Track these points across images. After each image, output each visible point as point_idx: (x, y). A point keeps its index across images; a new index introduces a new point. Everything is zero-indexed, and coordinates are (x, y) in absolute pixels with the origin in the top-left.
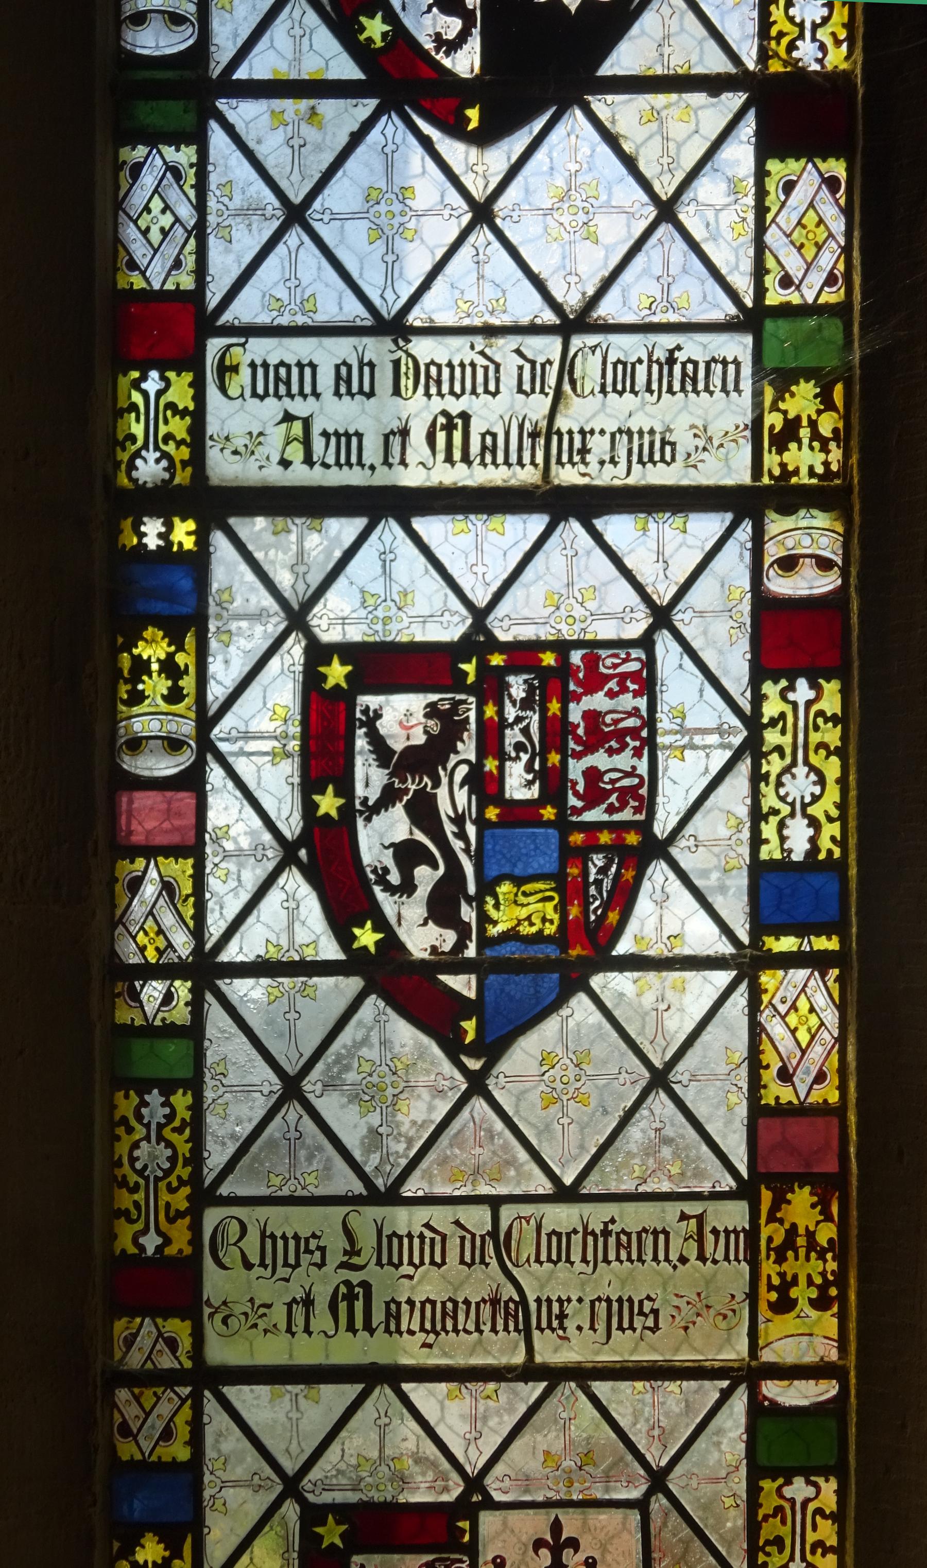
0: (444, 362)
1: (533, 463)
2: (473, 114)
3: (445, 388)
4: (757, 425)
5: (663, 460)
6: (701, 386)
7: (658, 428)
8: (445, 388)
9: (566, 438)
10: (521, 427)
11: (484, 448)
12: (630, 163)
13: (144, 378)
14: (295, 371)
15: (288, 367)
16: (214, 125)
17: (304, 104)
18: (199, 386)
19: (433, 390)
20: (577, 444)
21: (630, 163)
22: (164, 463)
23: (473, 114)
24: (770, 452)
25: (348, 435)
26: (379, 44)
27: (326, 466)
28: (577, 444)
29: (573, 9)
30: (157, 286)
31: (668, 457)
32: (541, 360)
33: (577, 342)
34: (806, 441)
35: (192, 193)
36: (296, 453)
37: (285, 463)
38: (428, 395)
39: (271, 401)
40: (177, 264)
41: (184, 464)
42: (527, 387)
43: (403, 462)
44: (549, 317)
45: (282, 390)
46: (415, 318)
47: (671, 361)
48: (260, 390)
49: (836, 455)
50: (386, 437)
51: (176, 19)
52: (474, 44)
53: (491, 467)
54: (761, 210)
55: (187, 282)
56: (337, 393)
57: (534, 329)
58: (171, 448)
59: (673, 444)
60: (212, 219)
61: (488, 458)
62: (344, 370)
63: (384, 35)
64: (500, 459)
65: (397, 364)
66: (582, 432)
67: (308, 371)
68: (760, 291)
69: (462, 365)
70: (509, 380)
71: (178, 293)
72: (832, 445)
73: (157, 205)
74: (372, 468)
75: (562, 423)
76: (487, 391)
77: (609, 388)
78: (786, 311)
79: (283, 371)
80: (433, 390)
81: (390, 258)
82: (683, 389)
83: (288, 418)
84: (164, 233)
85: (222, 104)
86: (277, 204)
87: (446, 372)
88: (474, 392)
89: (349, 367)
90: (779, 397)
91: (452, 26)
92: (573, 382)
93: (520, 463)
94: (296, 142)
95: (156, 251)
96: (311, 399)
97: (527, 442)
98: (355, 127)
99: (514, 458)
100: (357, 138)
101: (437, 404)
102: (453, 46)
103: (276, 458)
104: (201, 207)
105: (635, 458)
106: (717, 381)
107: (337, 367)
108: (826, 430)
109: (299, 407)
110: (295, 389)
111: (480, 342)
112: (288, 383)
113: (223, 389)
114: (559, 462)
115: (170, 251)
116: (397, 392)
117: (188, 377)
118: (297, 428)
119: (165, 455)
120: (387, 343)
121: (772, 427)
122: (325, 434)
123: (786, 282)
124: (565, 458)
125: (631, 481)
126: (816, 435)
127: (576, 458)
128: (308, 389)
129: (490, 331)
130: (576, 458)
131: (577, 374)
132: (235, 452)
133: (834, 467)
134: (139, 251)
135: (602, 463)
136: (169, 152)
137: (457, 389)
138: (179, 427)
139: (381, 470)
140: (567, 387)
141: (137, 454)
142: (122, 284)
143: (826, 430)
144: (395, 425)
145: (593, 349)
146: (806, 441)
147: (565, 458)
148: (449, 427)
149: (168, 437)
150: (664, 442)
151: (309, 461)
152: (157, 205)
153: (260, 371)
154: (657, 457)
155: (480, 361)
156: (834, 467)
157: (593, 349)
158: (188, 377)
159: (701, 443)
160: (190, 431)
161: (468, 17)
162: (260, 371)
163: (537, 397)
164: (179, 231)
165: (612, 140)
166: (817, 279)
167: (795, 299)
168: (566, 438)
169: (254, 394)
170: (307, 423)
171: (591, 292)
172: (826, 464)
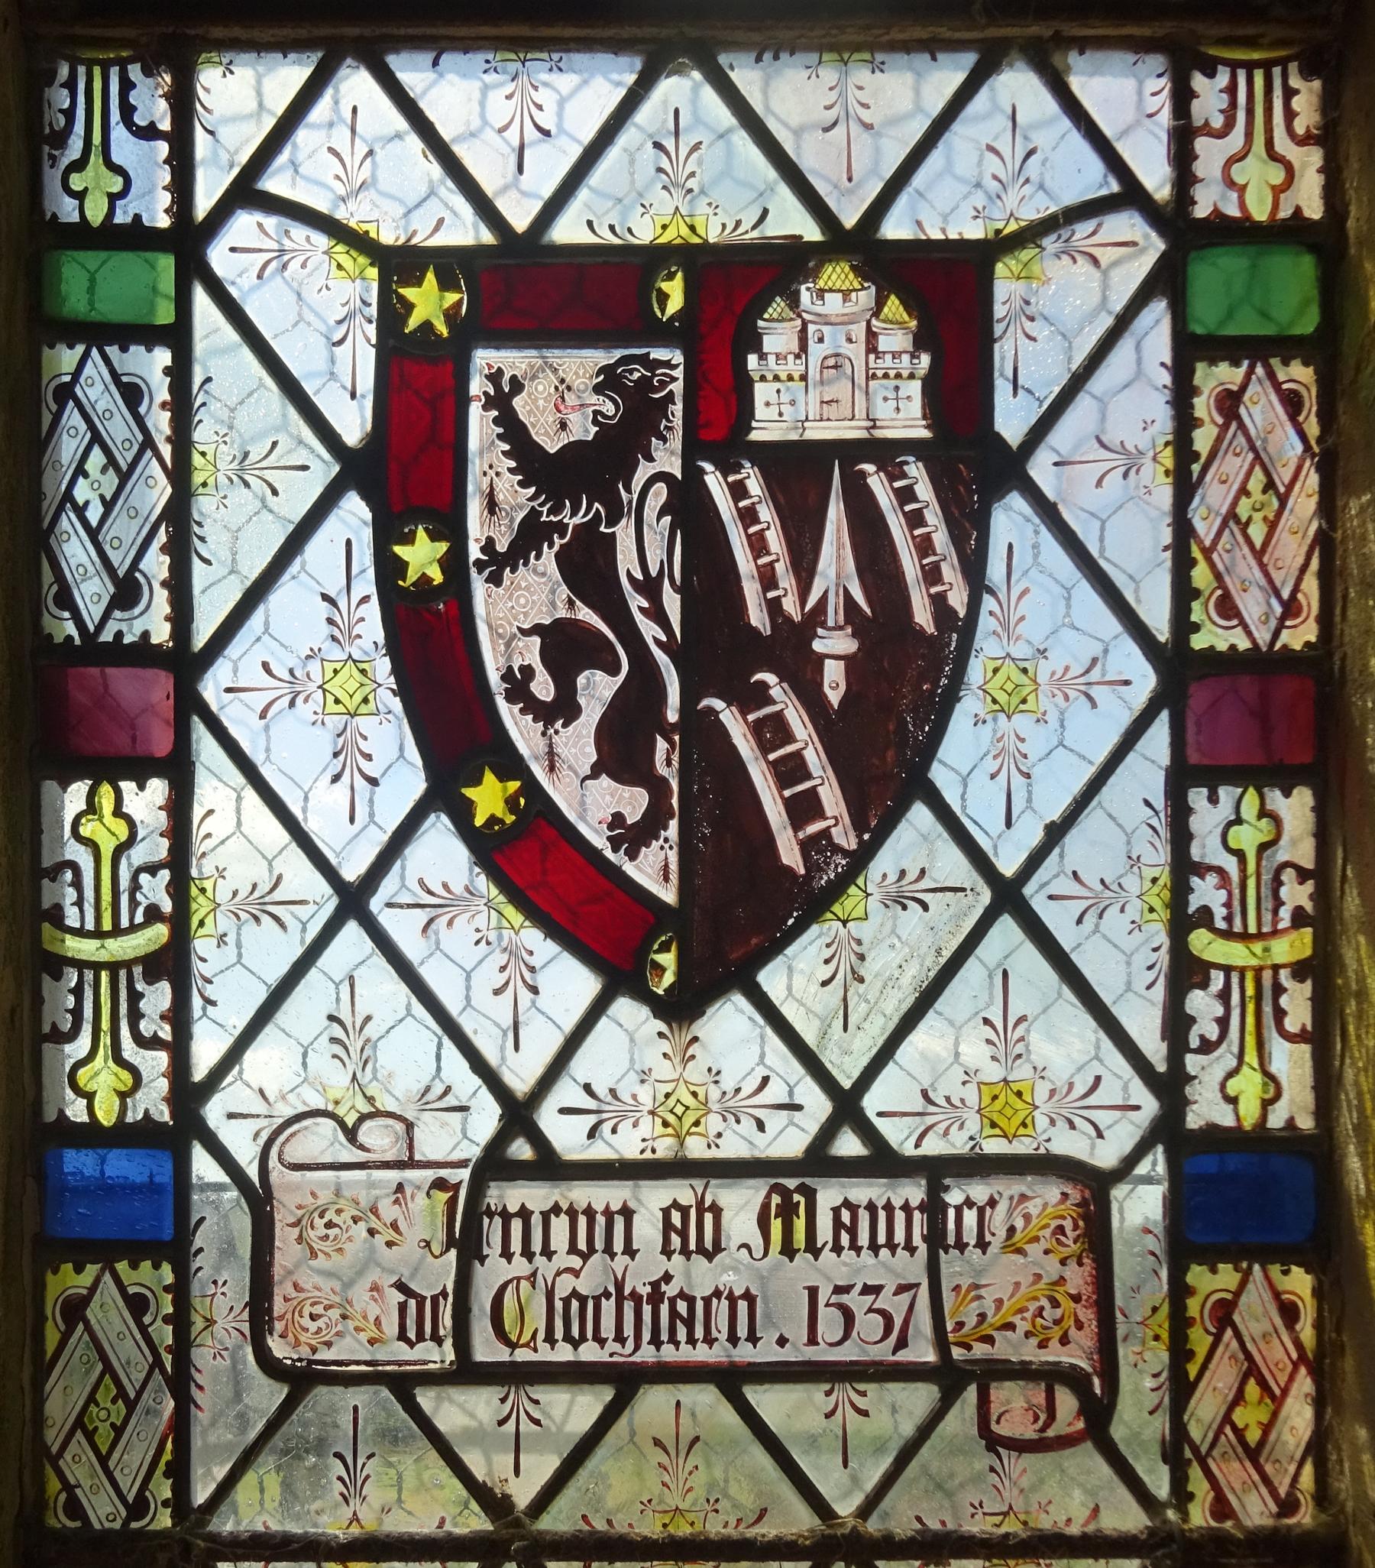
91: (634, 803)
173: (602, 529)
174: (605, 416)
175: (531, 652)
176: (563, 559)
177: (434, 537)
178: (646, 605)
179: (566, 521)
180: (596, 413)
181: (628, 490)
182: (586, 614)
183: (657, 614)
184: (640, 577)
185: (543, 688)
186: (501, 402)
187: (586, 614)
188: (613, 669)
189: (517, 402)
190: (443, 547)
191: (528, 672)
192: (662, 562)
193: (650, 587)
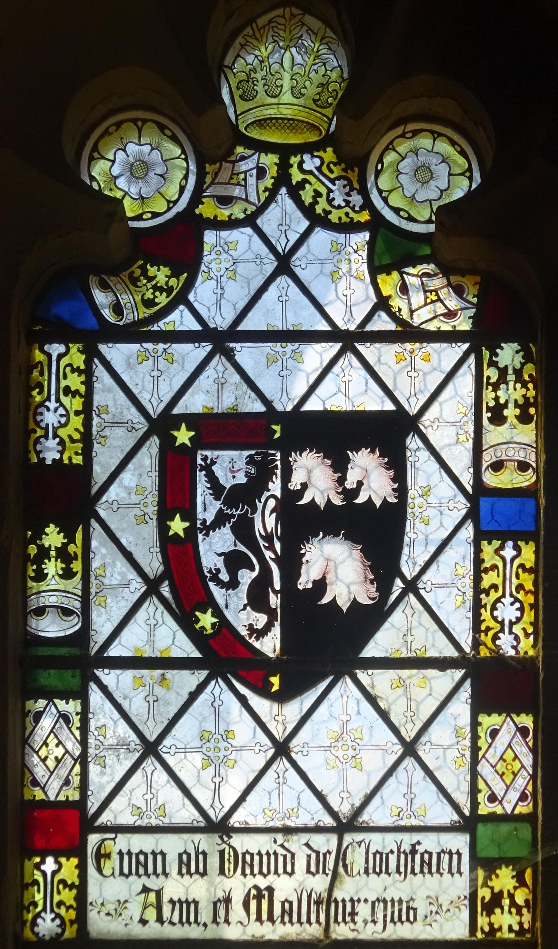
0: (255, 851)
1: (318, 921)
2: (275, 681)
3: (256, 870)
4: (473, 897)
5: (408, 919)
6: (434, 869)
7: (405, 899)
8: (256, 870)
9: (341, 905)
10: (309, 897)
11: (283, 911)
12: (384, 715)
13: (43, 862)
14: (150, 858)
15: (146, 855)
16: (93, 686)
17: (157, 673)
18: (82, 868)
19: (248, 871)
20: (349, 909)
21: (384, 715)
22: (58, 922)
23: (275, 681)
24: (482, 914)
25: (188, 903)
26: (210, 631)
27: (172, 923)
28: (349, 909)
29: (345, 609)
30: (52, 798)
31: (412, 918)
32: (323, 850)
33: (348, 838)
34: (506, 908)
35: (77, 733)
36: (151, 914)
37: (143, 922)
38: (244, 874)
39: (133, 878)
40: (67, 782)
41: (72, 922)
42: (313, 869)
43: (227, 921)
44: (328, 821)
45: (141, 871)
46: (235, 820)
47: (414, 852)
48: (126, 871)
49: (527, 917)
50: (215, 904)
51: (67, 612)
52: (276, 630)
53: (288, 925)
54: (475, 749)
55: (74, 796)
56: (180, 873)
57: (318, 829)
58: (62, 911)
59: (415, 910)
60: (91, 751)
61: (286, 919)
62: (185, 857)
63: (213, 625)
64: (295, 918)
65: (222, 853)
66: (352, 900)
67: (159, 858)
68: (475, 804)
69: (268, 854)
70: (301, 864)
71: (67, 803)
72: (525, 911)
73: (52, 742)
74: (205, 925)
75: (338, 894)
76: (285, 872)
77: (371, 871)
78: (492, 818)
79: (142, 858)
80: (248, 871)
81: (217, 780)
82: (422, 871)
83: (145, 890)
84: (58, 761)
85: (99, 673)
86: (138, 741)
87: (256, 858)
88: (276, 872)
89: (189, 855)
90: (488, 877)
91: (261, 620)
92: (345, 866)
93: (309, 921)
94: (151, 699)
95: (52, 773)
96: (162, 877)
97: (313, 908)
98: (193, 688)
99: (304, 918)
100: (193, 696)
101: (250, 881)
102: (261, 633)
103: (137, 918)
104: (84, 742)
105: (389, 918)
106: (445, 865)
107: (180, 855)
108: (520, 899)
109: (153, 883)
110: (150, 869)
111: (280, 838)
112: (146, 866)
113: (99, 870)
114: (336, 921)
115: (63, 772)
116: (222, 872)
117: (74, 861)
118: (152, 897)
119: (58, 916)
120: (216, 838)
121: (483, 898)
122: (172, 901)
123: (492, 798)
124: (340, 918)
125: (385, 936)
126: (513, 903)
127: (348, 919)
128: (159, 870)
129: (287, 831)
130: (348, 919)
131: (348, 861)
132: (108, 914)
133: (526, 926)
134: (40, 772)
135: (365, 922)
136: (61, 704)
137: (265, 870)
138: (68, 896)
139: (211, 926)
140: (341, 869)
141: (38, 915)
142: (27, 796)
143: (520, 899)
144: (220, 895)
145: (359, 844)
146: (506, 908)
147: (340, 918)
148: (259, 897)
149: (60, 903)
150: (408, 908)
151: (160, 919)
152: (52, 742)
153: (126, 858)
154: (404, 918)
155: (281, 851)
156: (526, 926)
157: (359, 844)
158: (74, 861)
159: (434, 909)
160: (76, 899)
161: (271, 613)
162: (126, 858)
163: (320, 877)
164: (69, 762)
165: (372, 700)
166: (514, 796)
167: (499, 810)
168: (341, 905)
169: (122, 873)
170: (159, 894)
171: (357, 804)
172: (521, 924)
173: (249, 516)
174: (250, 473)
175: (220, 563)
176: (233, 529)
177: (183, 520)
178: (267, 545)
179: (234, 513)
180: (246, 472)
181: (260, 502)
182: (242, 548)
183: (271, 548)
184: (264, 534)
185: (224, 576)
186: (208, 469)
187: (242, 548)
188: (252, 569)
189: (214, 468)
190: (187, 524)
191: (218, 571)
192: (272, 528)
193: (268, 538)
